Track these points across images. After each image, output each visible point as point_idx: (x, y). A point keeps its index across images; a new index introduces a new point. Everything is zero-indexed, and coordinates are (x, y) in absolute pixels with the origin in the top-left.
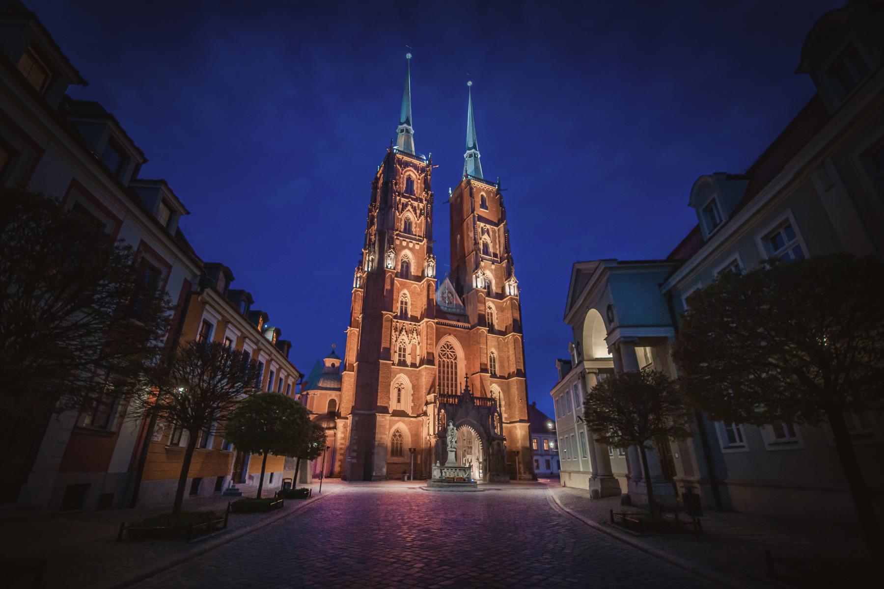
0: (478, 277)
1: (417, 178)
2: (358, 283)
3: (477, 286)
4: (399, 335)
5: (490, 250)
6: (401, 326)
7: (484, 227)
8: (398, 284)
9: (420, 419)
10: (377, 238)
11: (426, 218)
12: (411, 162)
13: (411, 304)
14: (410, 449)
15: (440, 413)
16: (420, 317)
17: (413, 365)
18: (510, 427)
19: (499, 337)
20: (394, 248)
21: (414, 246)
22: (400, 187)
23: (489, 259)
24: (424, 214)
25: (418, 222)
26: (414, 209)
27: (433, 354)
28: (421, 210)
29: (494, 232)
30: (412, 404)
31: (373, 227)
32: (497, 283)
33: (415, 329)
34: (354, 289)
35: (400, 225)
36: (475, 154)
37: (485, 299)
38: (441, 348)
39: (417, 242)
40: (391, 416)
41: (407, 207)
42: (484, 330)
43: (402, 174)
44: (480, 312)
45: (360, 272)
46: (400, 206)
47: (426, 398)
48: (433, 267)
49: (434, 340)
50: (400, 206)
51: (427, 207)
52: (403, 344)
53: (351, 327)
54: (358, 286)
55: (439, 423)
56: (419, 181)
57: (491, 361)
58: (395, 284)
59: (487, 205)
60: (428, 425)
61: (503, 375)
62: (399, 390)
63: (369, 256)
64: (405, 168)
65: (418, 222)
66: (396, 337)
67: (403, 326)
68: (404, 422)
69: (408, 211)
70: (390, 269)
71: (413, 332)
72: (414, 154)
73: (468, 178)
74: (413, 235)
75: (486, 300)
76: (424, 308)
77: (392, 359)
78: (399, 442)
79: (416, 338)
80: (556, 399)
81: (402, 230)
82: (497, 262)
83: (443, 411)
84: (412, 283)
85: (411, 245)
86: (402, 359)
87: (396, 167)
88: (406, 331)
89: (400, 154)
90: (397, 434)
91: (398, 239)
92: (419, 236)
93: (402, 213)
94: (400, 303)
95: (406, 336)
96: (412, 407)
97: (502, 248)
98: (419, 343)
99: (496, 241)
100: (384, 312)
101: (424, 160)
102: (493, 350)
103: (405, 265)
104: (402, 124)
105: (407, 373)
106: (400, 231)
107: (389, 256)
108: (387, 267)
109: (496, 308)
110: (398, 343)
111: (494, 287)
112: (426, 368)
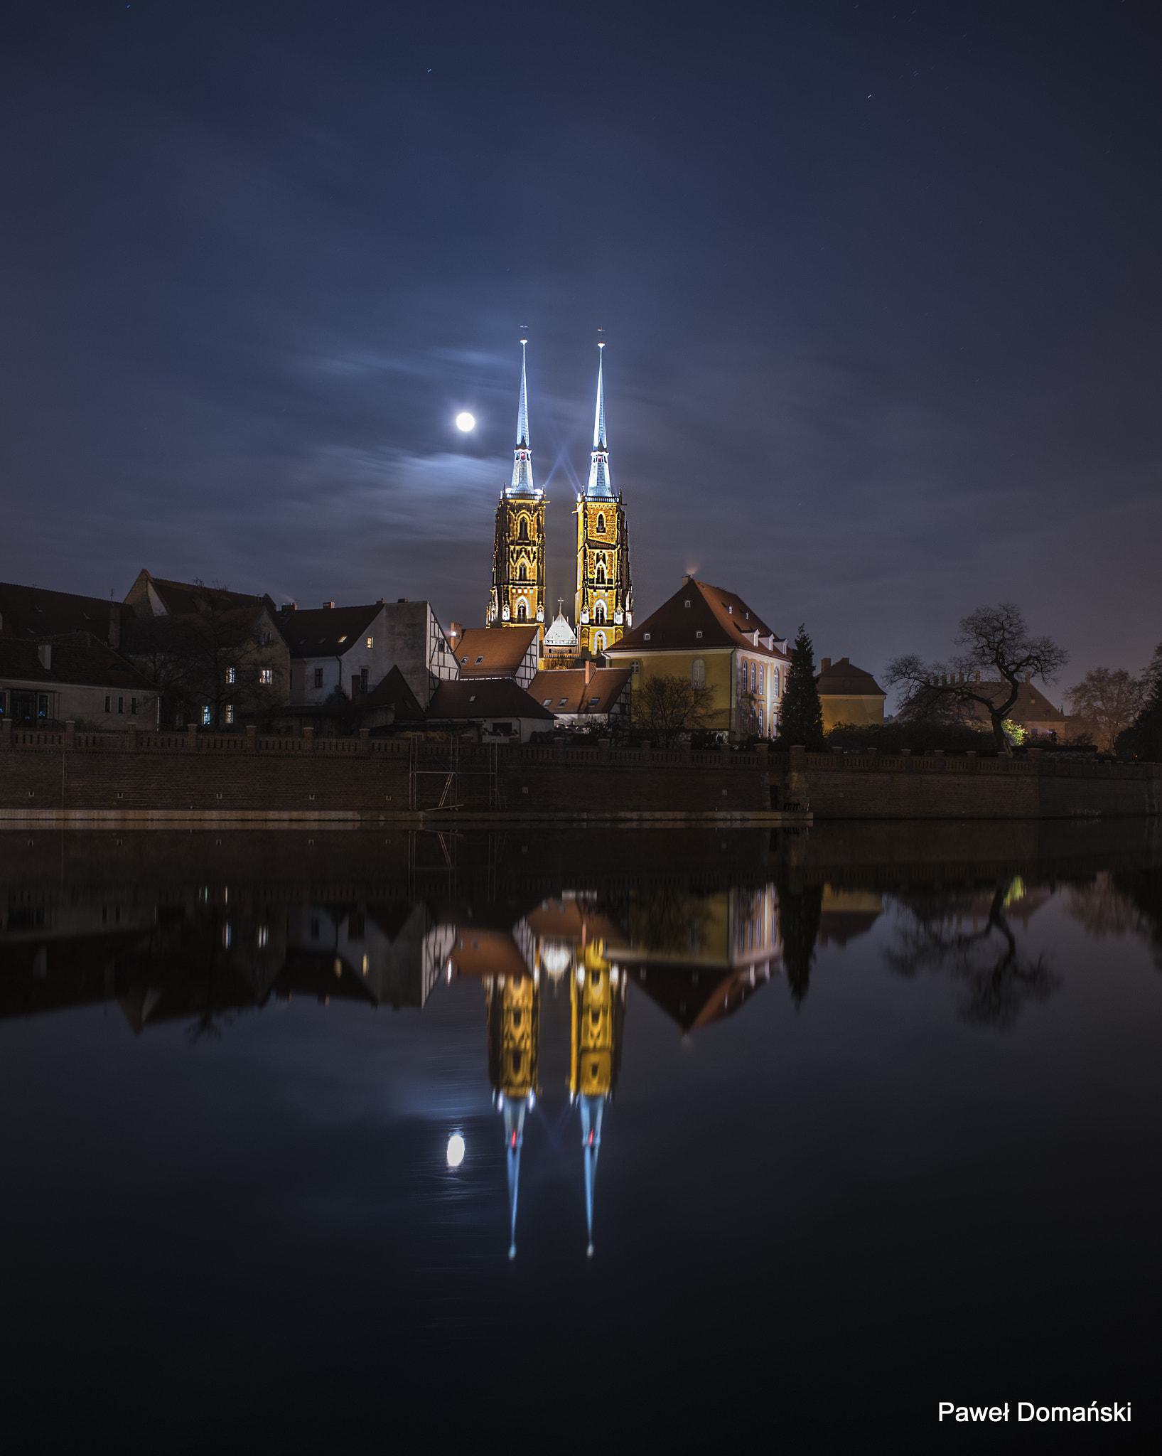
11: (538, 562)
21: (528, 591)
26: (528, 553)
29: (611, 555)
46: (515, 555)
50: (515, 555)
51: (538, 551)
56: (532, 523)
74: (527, 580)
82: (611, 588)
85: (526, 591)
103: (522, 609)
104: (518, 447)
106: (516, 580)
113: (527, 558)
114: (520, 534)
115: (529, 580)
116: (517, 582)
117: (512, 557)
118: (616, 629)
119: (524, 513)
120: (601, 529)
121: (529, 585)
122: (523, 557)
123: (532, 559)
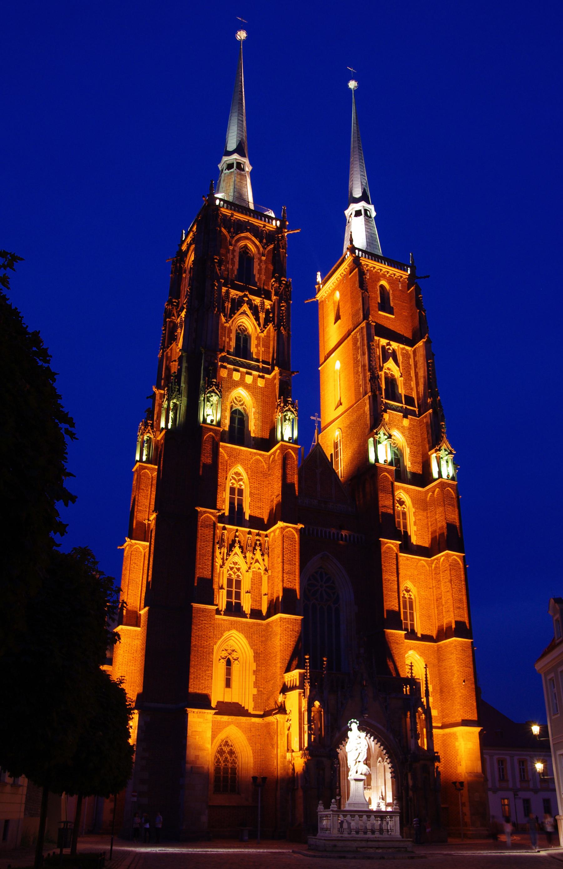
0: (380, 443)
2: (145, 452)
3: (377, 460)
4: (228, 555)
5: (400, 392)
6: (232, 537)
8: (225, 455)
9: (271, 719)
10: (184, 365)
13: (251, 493)
14: (254, 778)
15: (313, 709)
16: (268, 520)
17: (256, 614)
18: (444, 735)
19: (421, 560)
20: (217, 385)
21: (255, 380)
22: (227, 269)
23: (398, 407)
24: (273, 320)
25: (262, 335)
26: (255, 311)
28: (267, 312)
29: (406, 355)
30: (255, 691)
31: (174, 344)
32: (413, 454)
33: (258, 542)
34: (138, 464)
35: (227, 340)
36: (366, 211)
37: (392, 484)
39: (261, 374)
40: (216, 714)
41: (241, 306)
42: (392, 544)
43: (232, 245)
44: (384, 510)
45: (149, 432)
46: (228, 305)
47: (283, 678)
48: (293, 422)
49: (297, 564)
50: (228, 305)
52: (234, 573)
53: (131, 538)
54: (144, 458)
55: (310, 728)
56: (264, 258)
57: (405, 607)
58: (220, 454)
59: (392, 304)
60: (287, 732)
61: (428, 633)
62: (229, 663)
63: (169, 400)
64: (237, 234)
65: (262, 335)
66: (223, 559)
67: (236, 536)
68: (238, 725)
69: (242, 313)
70: (211, 425)
71: (254, 549)
72: (252, 207)
73: (355, 253)
74: (252, 359)
75: (395, 488)
76: (275, 502)
77: (215, 603)
78: (230, 765)
79: (260, 560)
80: (549, 677)
81: (232, 350)
82: (413, 413)
83: (317, 703)
84: (251, 453)
85: (249, 379)
86: (234, 601)
87: (221, 231)
88: (241, 547)
89: (227, 208)
90: (226, 749)
91: (225, 367)
92: (264, 362)
93: (231, 317)
95: (241, 556)
96: (254, 695)
97: (421, 388)
98: (266, 570)
99: (410, 374)
100: (199, 509)
101: (272, 219)
102: (409, 584)
103: (237, 417)
104: (230, 153)
105: (241, 629)
107: (209, 401)
108: (205, 420)
109: (414, 504)
110: (225, 571)
111: (408, 463)
112: (281, 618)
114: (239, 270)
115: (257, 360)
117: (223, 309)
119: (247, 238)
121: (257, 369)
123: (262, 321)
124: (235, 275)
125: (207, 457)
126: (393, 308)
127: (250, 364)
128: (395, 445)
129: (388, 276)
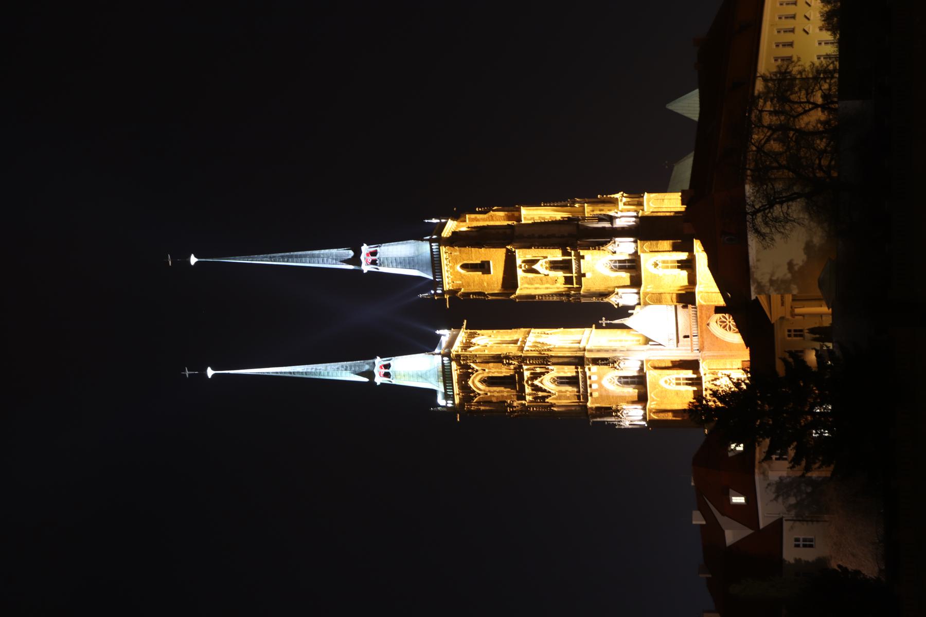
1: (483, 373)
7: (523, 268)
12: (459, 382)
21: (594, 374)
26: (535, 376)
27: (743, 361)
35: (568, 393)
38: (726, 330)
41: (537, 386)
43: (486, 394)
46: (540, 394)
50: (540, 394)
56: (487, 370)
81: (575, 390)
85: (594, 378)
88: (716, 379)
93: (549, 392)
94: (679, 388)
106: (579, 392)
113: (543, 377)
115: (577, 372)
116: (581, 390)
117: (544, 398)
118: (644, 252)
119: (473, 382)
120: (484, 267)
122: (541, 382)
123: (543, 370)
124: (512, 389)
125: (668, 415)
126: (482, 261)
127: (582, 378)
128: (608, 264)
129: (450, 264)
